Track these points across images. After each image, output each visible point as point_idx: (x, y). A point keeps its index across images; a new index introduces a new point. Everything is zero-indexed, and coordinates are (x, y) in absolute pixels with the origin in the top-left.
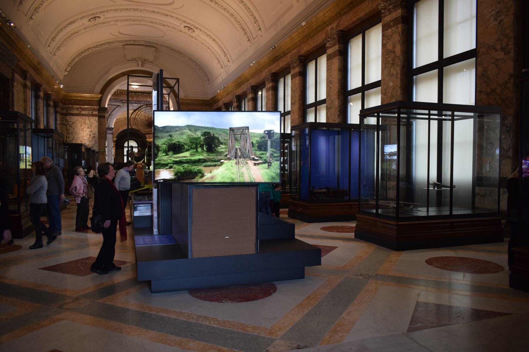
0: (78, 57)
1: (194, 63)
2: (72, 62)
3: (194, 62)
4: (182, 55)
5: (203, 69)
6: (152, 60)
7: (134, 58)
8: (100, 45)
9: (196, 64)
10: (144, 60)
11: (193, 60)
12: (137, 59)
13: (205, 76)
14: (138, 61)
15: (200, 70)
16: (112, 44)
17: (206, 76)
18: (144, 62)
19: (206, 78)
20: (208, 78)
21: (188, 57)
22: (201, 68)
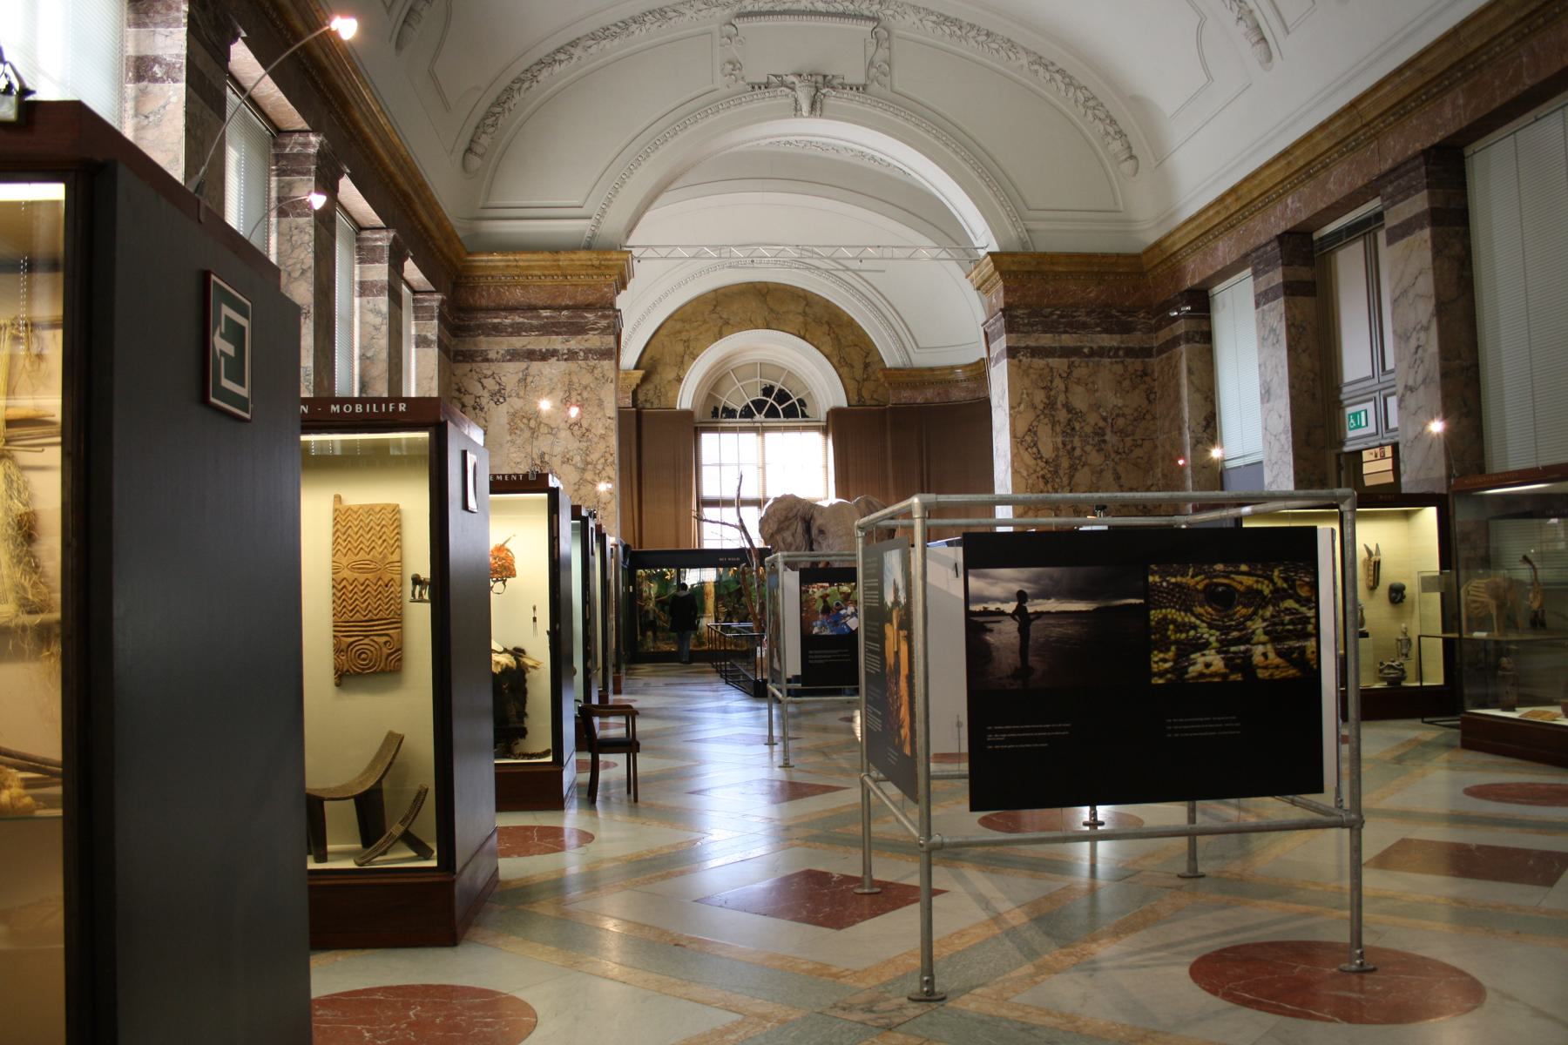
0: (523, 81)
1: (1058, 77)
2: (499, 110)
3: (1057, 72)
4: (994, 41)
5: (1102, 105)
6: (859, 79)
7: (775, 76)
8: (619, 27)
9: (1070, 82)
10: (820, 79)
11: (1053, 64)
12: (793, 79)
13: (1114, 139)
14: (793, 89)
15: (1086, 107)
16: (671, 14)
17: (1121, 134)
18: (824, 91)
19: (1117, 146)
20: (1129, 148)
21: (1027, 52)
22: (1094, 98)
